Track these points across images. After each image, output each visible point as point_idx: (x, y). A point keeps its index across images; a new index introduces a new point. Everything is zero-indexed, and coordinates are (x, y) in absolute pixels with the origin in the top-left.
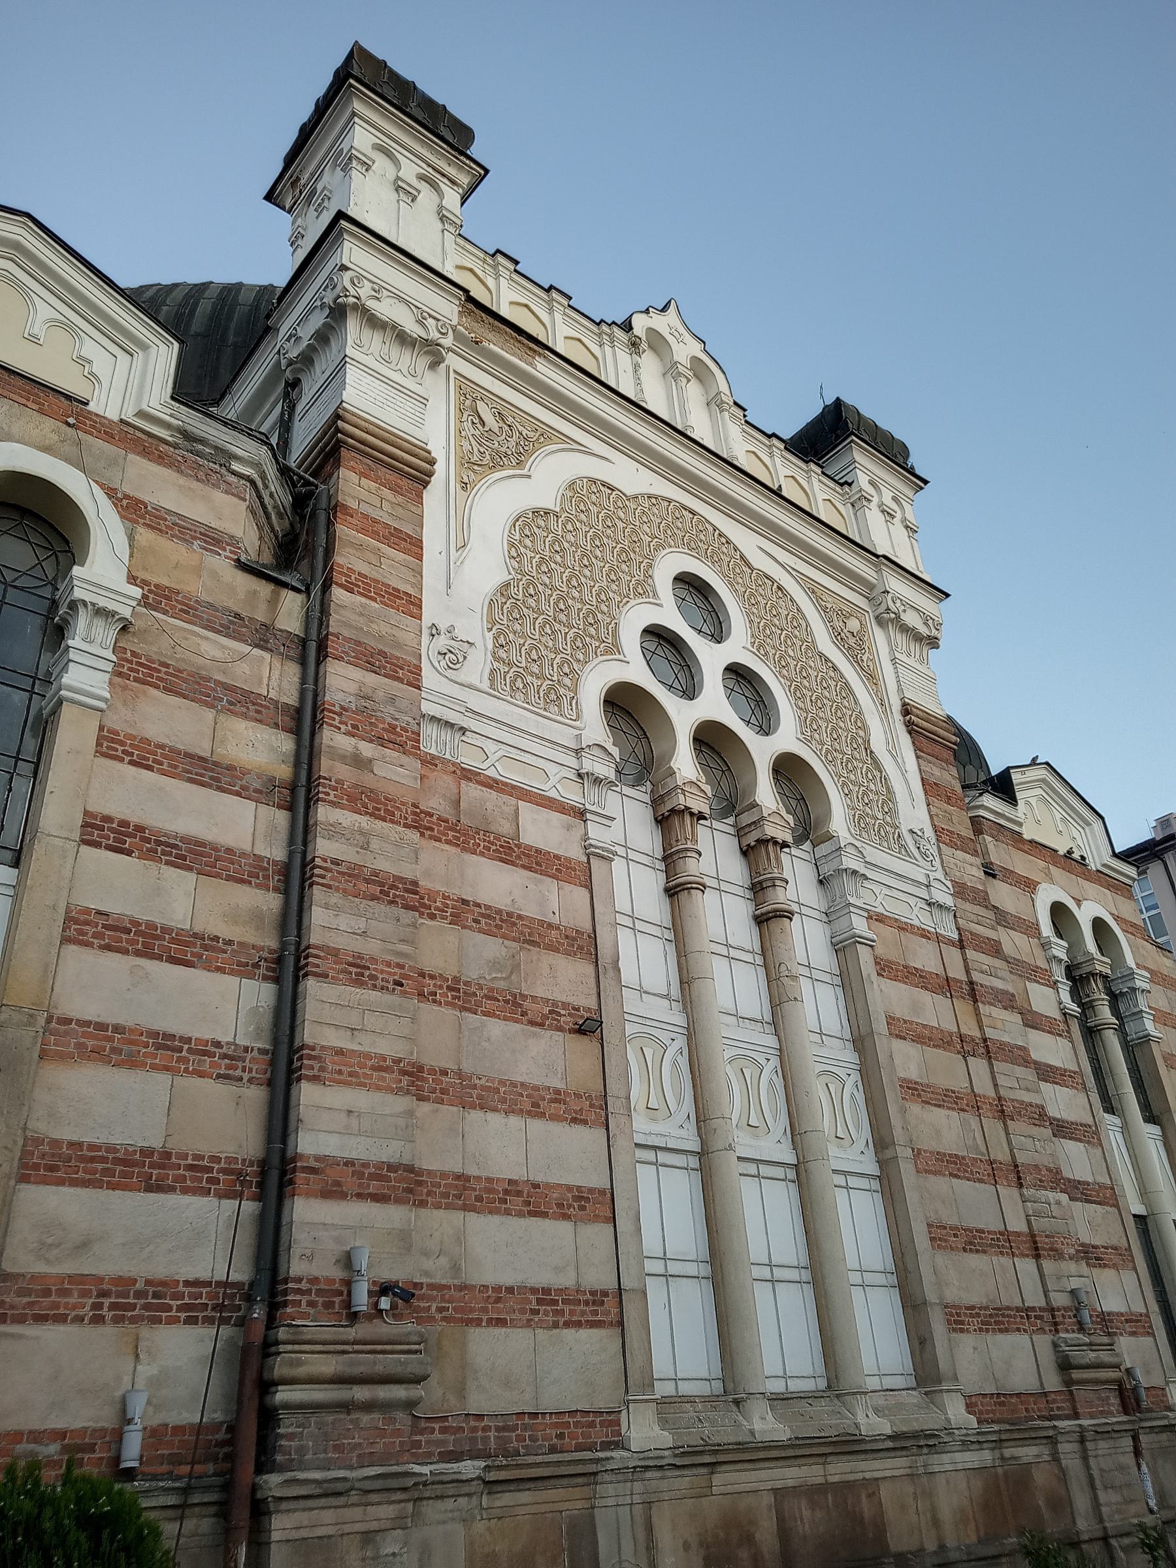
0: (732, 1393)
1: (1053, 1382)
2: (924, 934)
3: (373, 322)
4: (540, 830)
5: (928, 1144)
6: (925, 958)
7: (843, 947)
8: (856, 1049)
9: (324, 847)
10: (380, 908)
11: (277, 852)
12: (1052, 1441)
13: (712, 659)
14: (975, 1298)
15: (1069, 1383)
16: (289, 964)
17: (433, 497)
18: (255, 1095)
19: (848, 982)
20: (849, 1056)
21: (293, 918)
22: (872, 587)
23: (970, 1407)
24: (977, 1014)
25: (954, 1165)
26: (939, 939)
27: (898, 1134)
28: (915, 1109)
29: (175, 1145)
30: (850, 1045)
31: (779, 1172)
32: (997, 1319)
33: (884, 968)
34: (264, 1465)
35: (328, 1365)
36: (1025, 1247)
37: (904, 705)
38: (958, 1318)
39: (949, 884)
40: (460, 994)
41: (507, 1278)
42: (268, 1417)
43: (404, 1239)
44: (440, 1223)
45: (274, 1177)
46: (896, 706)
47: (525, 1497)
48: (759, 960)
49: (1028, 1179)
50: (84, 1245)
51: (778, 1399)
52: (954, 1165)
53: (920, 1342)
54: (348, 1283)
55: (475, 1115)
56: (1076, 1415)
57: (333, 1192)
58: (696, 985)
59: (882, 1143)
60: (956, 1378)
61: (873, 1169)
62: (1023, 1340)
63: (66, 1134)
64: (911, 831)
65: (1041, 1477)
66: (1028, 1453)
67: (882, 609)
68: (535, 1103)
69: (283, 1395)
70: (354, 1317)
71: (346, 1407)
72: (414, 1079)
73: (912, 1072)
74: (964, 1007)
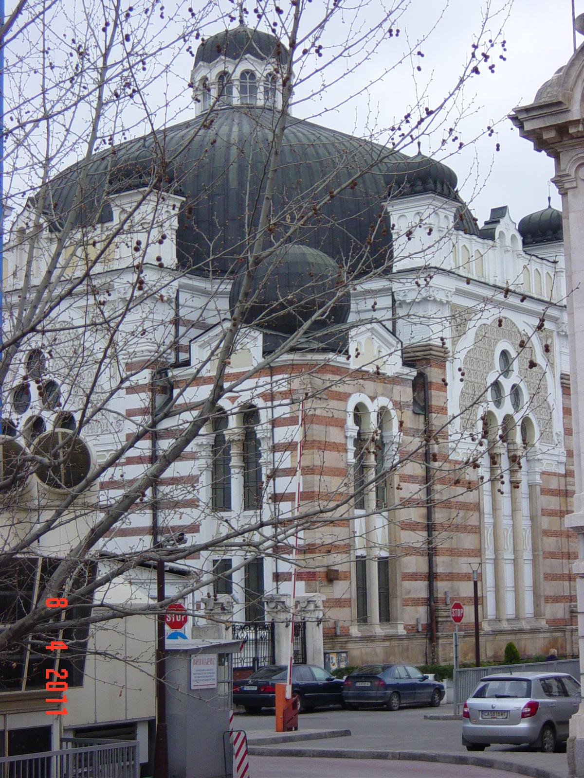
0: (498, 620)
1: (567, 616)
2: (555, 474)
3: (435, 301)
4: (470, 474)
5: (547, 549)
6: (554, 484)
7: (531, 486)
8: (531, 519)
9: (437, 497)
10: (445, 510)
11: (424, 497)
12: (565, 631)
13: (507, 384)
14: (552, 594)
15: (571, 616)
16: (430, 528)
17: (448, 364)
18: (427, 558)
19: (531, 497)
20: (529, 522)
21: (429, 516)
22: (557, 319)
23: (547, 622)
24: (566, 501)
25: (552, 555)
26: (559, 475)
27: (540, 548)
28: (545, 538)
29: (418, 571)
30: (529, 518)
31: (509, 562)
32: (556, 599)
33: (544, 492)
34: (437, 631)
35: (445, 614)
36: (567, 578)
37: (562, 374)
38: (547, 599)
39: (565, 452)
40: (458, 528)
41: (465, 595)
42: (437, 622)
43: (452, 588)
44: (456, 584)
45: (431, 577)
46: (558, 376)
47: (468, 639)
48: (510, 495)
49: (572, 557)
50: (410, 592)
51: (508, 620)
52: (552, 555)
53: (537, 605)
54: (446, 598)
55: (460, 558)
56: (572, 625)
57: (442, 580)
58: (498, 511)
59: (534, 549)
60: (544, 615)
61: (531, 558)
62: (562, 605)
63: (405, 571)
64: (557, 433)
65: (560, 640)
66: (559, 634)
67: (560, 330)
68: (470, 553)
69: (440, 619)
70: (447, 605)
71: (447, 621)
72: (454, 553)
73: (545, 526)
74: (563, 499)
